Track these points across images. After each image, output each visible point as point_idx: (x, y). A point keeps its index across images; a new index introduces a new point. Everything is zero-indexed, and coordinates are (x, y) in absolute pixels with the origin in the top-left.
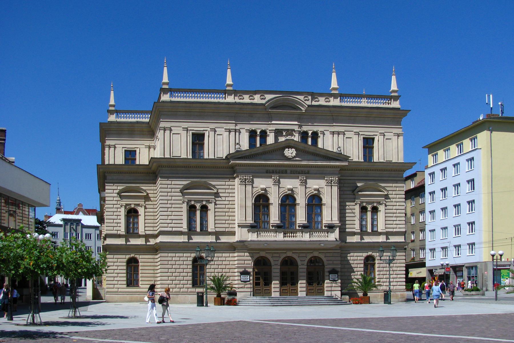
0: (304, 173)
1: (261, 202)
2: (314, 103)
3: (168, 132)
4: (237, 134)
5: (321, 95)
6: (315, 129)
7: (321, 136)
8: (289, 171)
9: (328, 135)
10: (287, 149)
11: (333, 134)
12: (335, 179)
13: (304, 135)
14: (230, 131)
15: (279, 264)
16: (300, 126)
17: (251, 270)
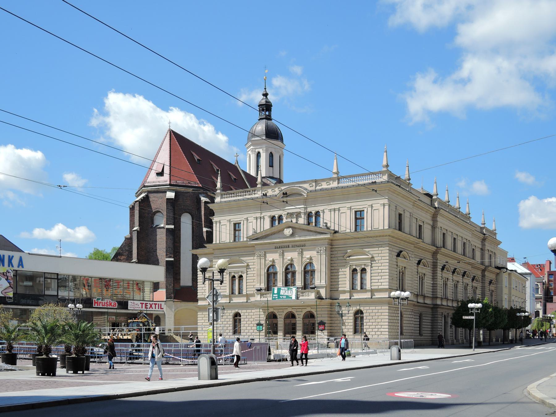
0: (301, 246)
2: (318, 188)
3: (218, 224)
4: (262, 220)
5: (323, 180)
7: (321, 214)
8: (290, 246)
9: (327, 213)
12: (323, 248)
13: (309, 215)
14: (257, 218)
15: (283, 317)
16: (306, 208)
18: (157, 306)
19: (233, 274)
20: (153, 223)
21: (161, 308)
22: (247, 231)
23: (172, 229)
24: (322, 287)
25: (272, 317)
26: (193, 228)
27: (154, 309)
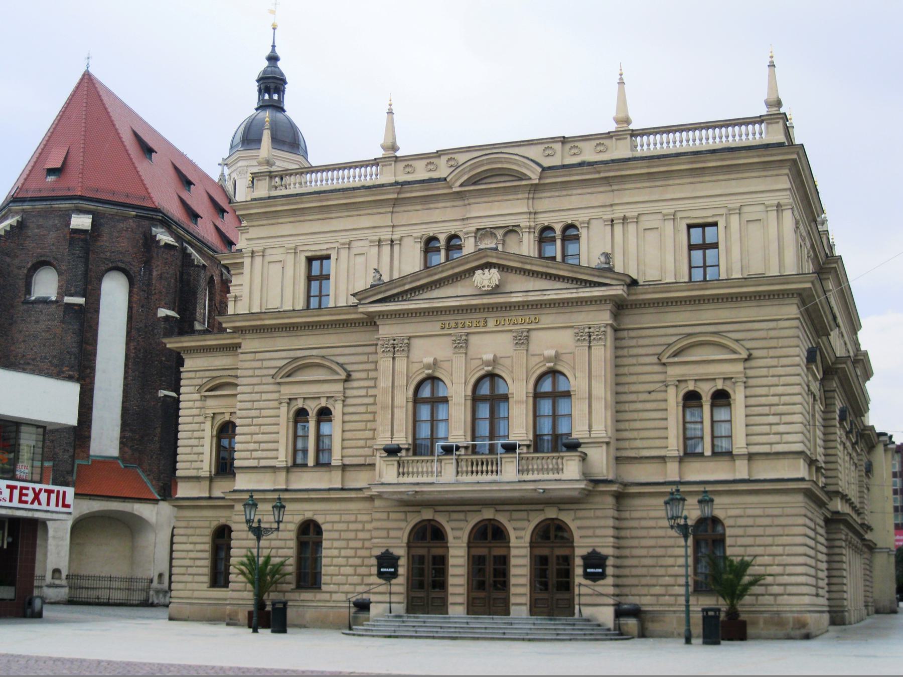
1: (428, 393)
4: (396, 248)
10: (480, 271)
11: (612, 225)
13: (545, 235)
18: (53, 497)
19: (300, 404)
20: (28, 291)
21: (64, 505)
22: (347, 282)
23: (80, 305)
24: (596, 443)
25: (429, 535)
26: (130, 308)
27: (44, 506)
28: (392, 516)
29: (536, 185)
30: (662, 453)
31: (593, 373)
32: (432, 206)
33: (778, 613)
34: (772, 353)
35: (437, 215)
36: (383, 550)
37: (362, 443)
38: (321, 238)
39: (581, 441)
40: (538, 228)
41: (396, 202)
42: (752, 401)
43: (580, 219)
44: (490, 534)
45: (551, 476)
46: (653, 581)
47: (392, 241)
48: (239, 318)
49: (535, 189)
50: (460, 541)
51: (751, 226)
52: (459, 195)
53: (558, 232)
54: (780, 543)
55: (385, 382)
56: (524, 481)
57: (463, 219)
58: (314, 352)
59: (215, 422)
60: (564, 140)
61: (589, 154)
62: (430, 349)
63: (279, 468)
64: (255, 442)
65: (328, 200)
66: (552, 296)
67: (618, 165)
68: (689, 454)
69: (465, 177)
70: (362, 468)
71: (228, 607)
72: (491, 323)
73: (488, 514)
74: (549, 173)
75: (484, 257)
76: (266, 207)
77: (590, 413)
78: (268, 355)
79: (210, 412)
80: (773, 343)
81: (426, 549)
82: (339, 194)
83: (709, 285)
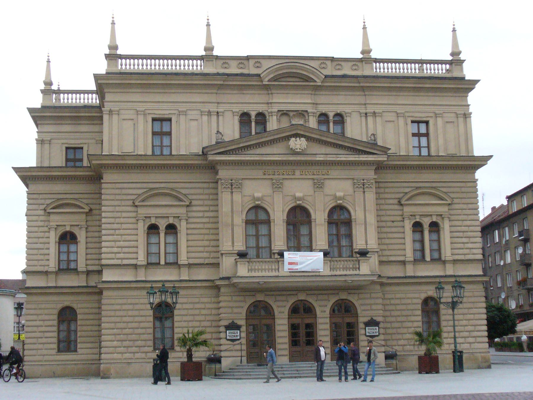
1: (257, 218)
4: (221, 118)
6: (339, 109)
13: (323, 118)
14: (209, 113)
17: (242, 322)
22: (191, 137)
28: (235, 298)
29: (320, 86)
30: (402, 258)
31: (367, 208)
32: (245, 92)
33: (473, 353)
34: (464, 201)
35: (247, 98)
36: (230, 321)
37: (201, 249)
38: (165, 106)
39: (370, 250)
40: (318, 113)
41: (221, 87)
42: (454, 229)
43: (346, 111)
44: (302, 310)
45: (351, 272)
46: (400, 336)
47: (218, 113)
48: (440, 158)
49: (317, 88)
50: (282, 314)
51: (448, 125)
52: (267, 88)
53: (253, 117)
54: (472, 312)
55: (225, 208)
56: (335, 275)
57: (268, 103)
58: (162, 185)
59: (57, 233)
60: (332, 59)
61: (347, 70)
62: (257, 189)
63: (140, 266)
64: (118, 247)
65: (171, 80)
66: (343, 158)
67: (360, 78)
68: (420, 259)
69: (272, 76)
70: (203, 266)
71: (69, 367)
72: (297, 173)
73: (302, 296)
74: (328, 79)
75: (295, 130)
76: (122, 80)
77: (366, 232)
78: (125, 185)
79: (53, 224)
80: (464, 195)
81: (300, 320)
82: (182, 77)
83: (432, 158)
